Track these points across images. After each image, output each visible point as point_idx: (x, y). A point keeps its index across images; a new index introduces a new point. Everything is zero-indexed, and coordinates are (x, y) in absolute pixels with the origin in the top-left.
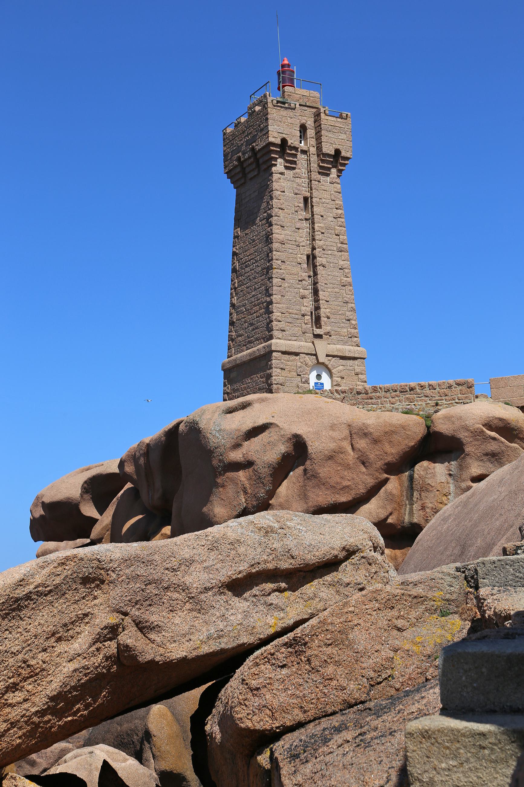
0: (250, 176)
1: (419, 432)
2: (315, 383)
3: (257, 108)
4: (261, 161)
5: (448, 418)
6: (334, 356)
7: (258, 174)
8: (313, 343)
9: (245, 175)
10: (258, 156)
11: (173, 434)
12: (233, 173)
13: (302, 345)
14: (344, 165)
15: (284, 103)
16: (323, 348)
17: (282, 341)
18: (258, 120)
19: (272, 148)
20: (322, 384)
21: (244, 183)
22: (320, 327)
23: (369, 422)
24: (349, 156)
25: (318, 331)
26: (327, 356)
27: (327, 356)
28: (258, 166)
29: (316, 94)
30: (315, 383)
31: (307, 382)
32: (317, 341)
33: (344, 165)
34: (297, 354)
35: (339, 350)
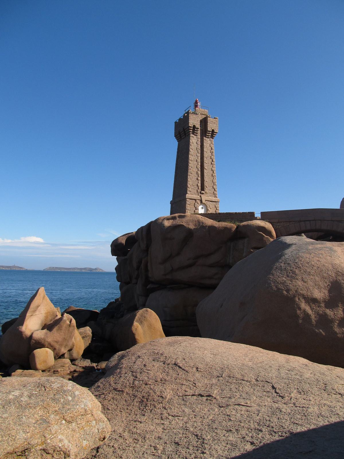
0: (182, 138)
1: (234, 229)
3: (186, 115)
4: (186, 133)
5: (244, 226)
6: (208, 201)
7: (185, 137)
8: (200, 196)
9: (181, 137)
10: (185, 131)
11: (150, 225)
12: (177, 137)
13: (197, 197)
14: (215, 135)
15: (195, 113)
16: (204, 198)
17: (190, 195)
18: (185, 119)
19: (190, 128)
21: (181, 140)
22: (203, 190)
23: (216, 226)
24: (217, 132)
26: (206, 200)
27: (206, 200)
28: (185, 134)
29: (207, 111)
32: (202, 196)
33: (215, 135)
35: (210, 199)
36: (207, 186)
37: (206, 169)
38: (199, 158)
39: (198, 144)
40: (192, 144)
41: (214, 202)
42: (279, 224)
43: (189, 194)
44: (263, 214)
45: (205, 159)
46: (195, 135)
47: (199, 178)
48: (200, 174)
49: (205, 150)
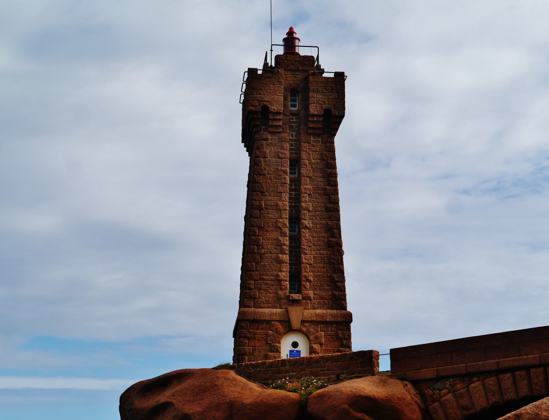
2: (290, 351)
5: (321, 397)
16: (296, 315)
20: (299, 351)
22: (299, 292)
25: (295, 296)
30: (290, 351)
31: (278, 351)
32: (290, 308)
34: (268, 322)
36: (311, 278)
37: (306, 227)
38: (286, 197)
39: (281, 158)
40: (262, 159)
41: (331, 323)
42: (439, 385)
43: (249, 307)
44: (396, 354)
45: (303, 199)
46: (273, 133)
47: (286, 258)
48: (288, 243)
49: (303, 171)
